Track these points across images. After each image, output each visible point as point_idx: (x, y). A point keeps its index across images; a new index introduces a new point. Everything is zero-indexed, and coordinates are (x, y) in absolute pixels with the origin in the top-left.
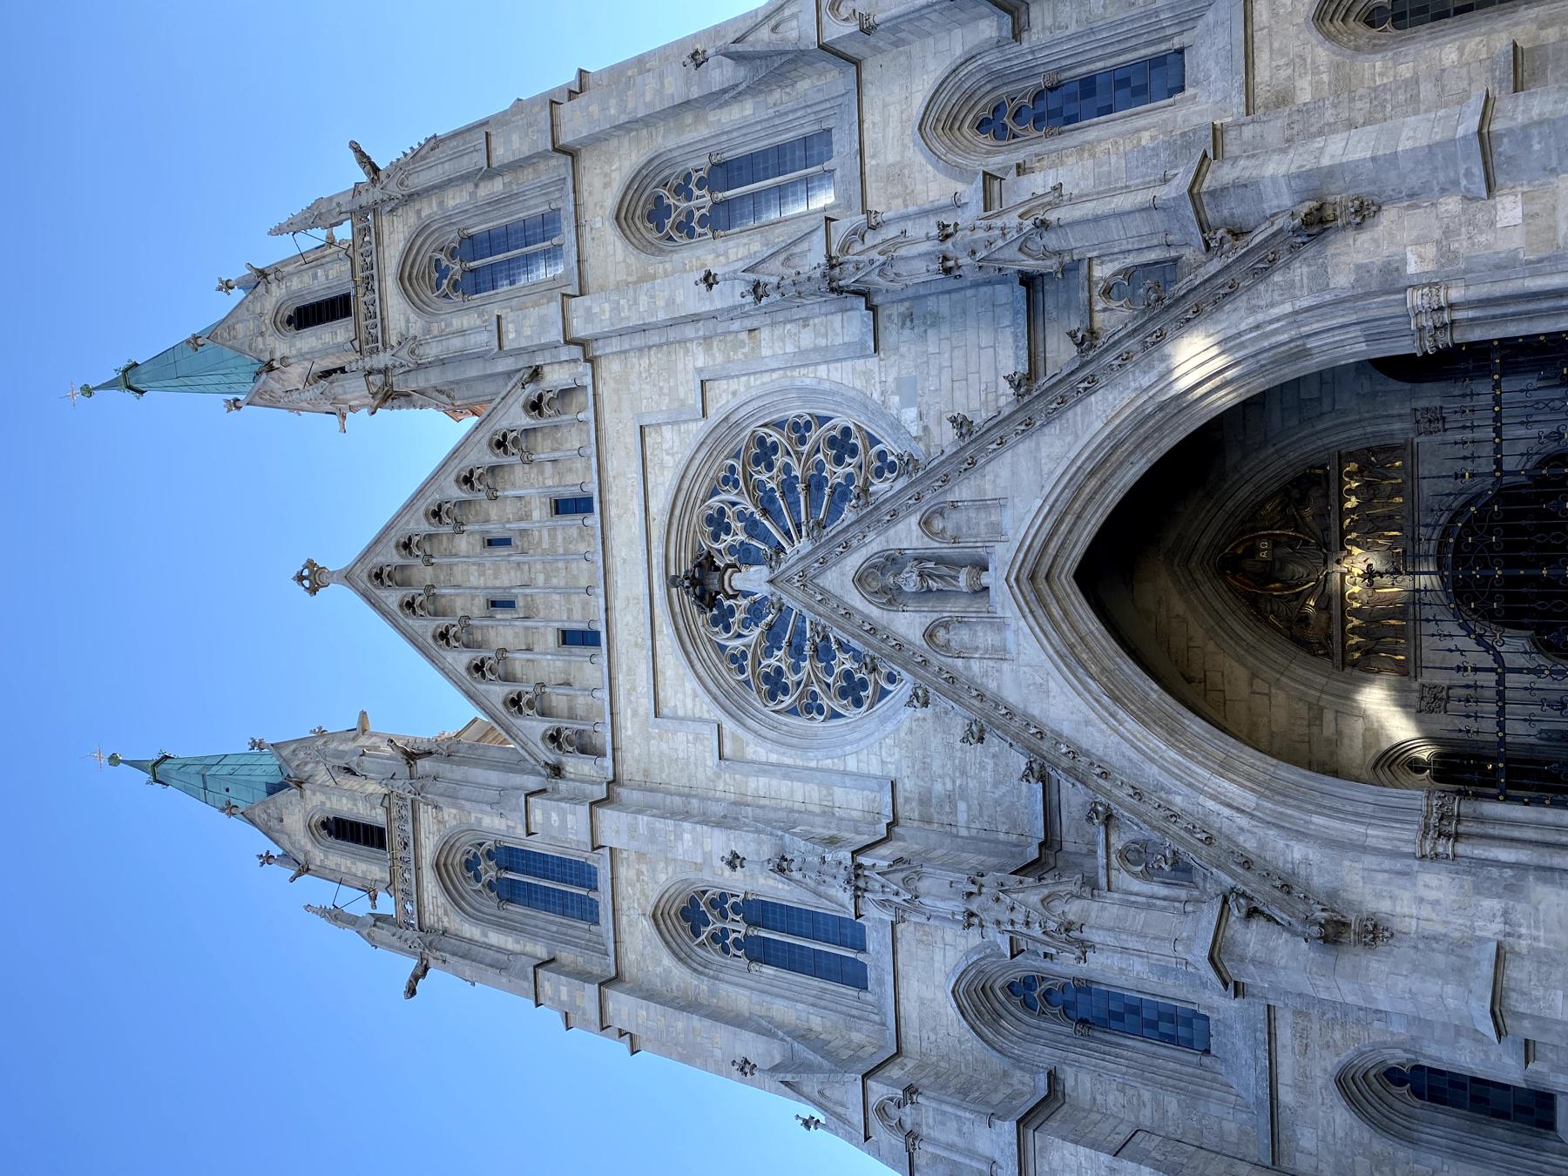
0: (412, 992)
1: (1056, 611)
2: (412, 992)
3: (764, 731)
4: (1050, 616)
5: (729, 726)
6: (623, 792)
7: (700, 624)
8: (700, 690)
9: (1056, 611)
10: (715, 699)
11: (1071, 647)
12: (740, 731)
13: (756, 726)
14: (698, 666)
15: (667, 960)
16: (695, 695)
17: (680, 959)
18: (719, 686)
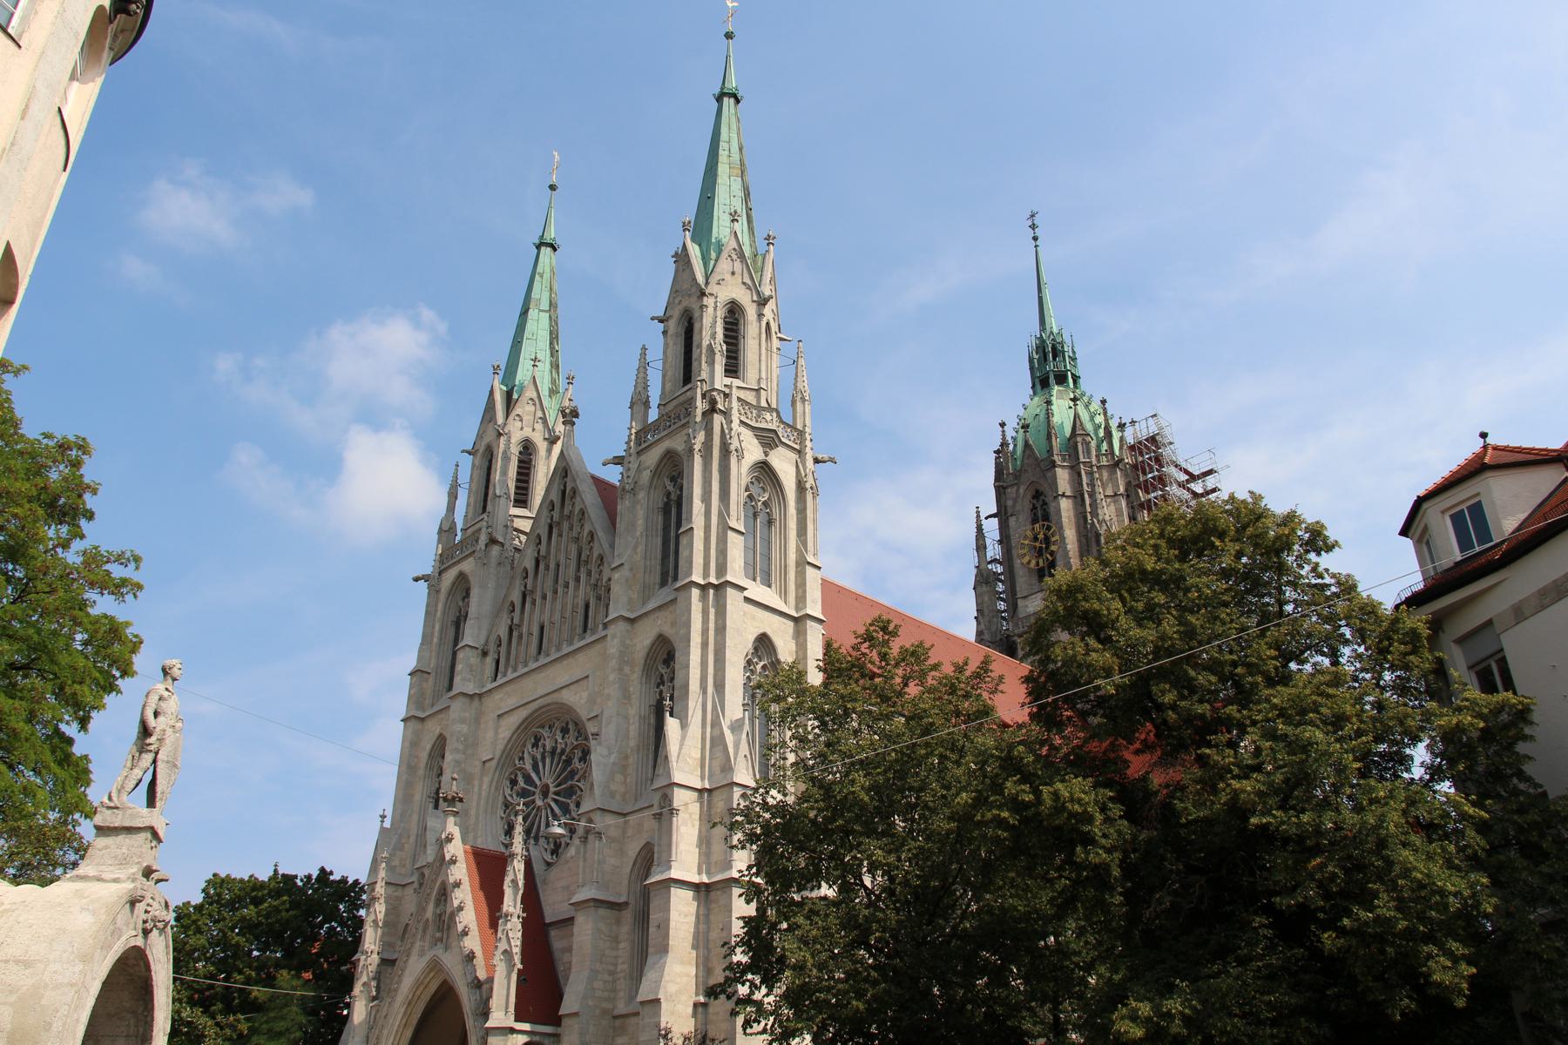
0: (416, 579)
1: (432, 975)
2: (416, 579)
3: (494, 783)
4: (429, 973)
5: (494, 763)
6: (476, 699)
7: (534, 729)
8: (505, 741)
9: (432, 975)
10: (503, 751)
11: (422, 983)
12: (492, 771)
13: (496, 778)
14: (516, 735)
15: (429, 747)
16: (504, 739)
17: (430, 755)
18: (511, 750)
